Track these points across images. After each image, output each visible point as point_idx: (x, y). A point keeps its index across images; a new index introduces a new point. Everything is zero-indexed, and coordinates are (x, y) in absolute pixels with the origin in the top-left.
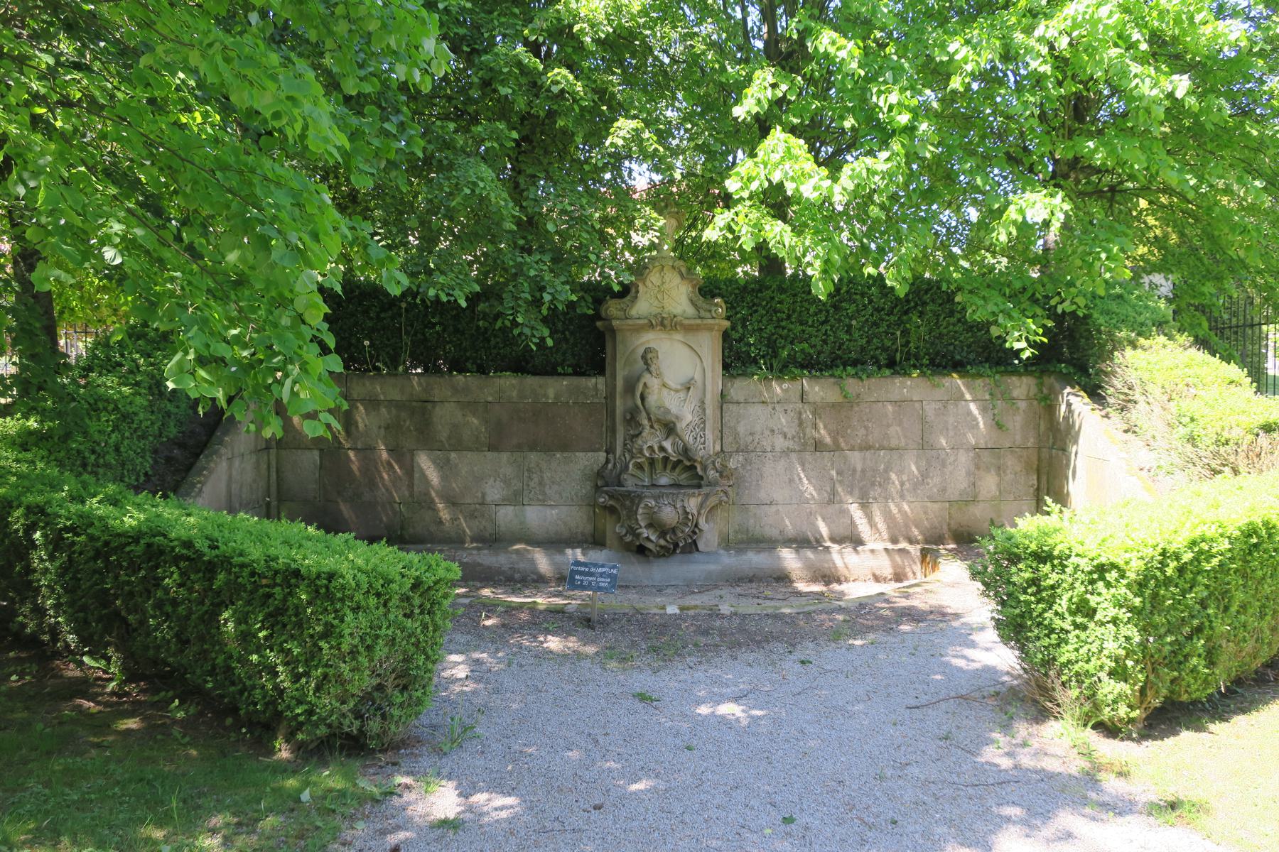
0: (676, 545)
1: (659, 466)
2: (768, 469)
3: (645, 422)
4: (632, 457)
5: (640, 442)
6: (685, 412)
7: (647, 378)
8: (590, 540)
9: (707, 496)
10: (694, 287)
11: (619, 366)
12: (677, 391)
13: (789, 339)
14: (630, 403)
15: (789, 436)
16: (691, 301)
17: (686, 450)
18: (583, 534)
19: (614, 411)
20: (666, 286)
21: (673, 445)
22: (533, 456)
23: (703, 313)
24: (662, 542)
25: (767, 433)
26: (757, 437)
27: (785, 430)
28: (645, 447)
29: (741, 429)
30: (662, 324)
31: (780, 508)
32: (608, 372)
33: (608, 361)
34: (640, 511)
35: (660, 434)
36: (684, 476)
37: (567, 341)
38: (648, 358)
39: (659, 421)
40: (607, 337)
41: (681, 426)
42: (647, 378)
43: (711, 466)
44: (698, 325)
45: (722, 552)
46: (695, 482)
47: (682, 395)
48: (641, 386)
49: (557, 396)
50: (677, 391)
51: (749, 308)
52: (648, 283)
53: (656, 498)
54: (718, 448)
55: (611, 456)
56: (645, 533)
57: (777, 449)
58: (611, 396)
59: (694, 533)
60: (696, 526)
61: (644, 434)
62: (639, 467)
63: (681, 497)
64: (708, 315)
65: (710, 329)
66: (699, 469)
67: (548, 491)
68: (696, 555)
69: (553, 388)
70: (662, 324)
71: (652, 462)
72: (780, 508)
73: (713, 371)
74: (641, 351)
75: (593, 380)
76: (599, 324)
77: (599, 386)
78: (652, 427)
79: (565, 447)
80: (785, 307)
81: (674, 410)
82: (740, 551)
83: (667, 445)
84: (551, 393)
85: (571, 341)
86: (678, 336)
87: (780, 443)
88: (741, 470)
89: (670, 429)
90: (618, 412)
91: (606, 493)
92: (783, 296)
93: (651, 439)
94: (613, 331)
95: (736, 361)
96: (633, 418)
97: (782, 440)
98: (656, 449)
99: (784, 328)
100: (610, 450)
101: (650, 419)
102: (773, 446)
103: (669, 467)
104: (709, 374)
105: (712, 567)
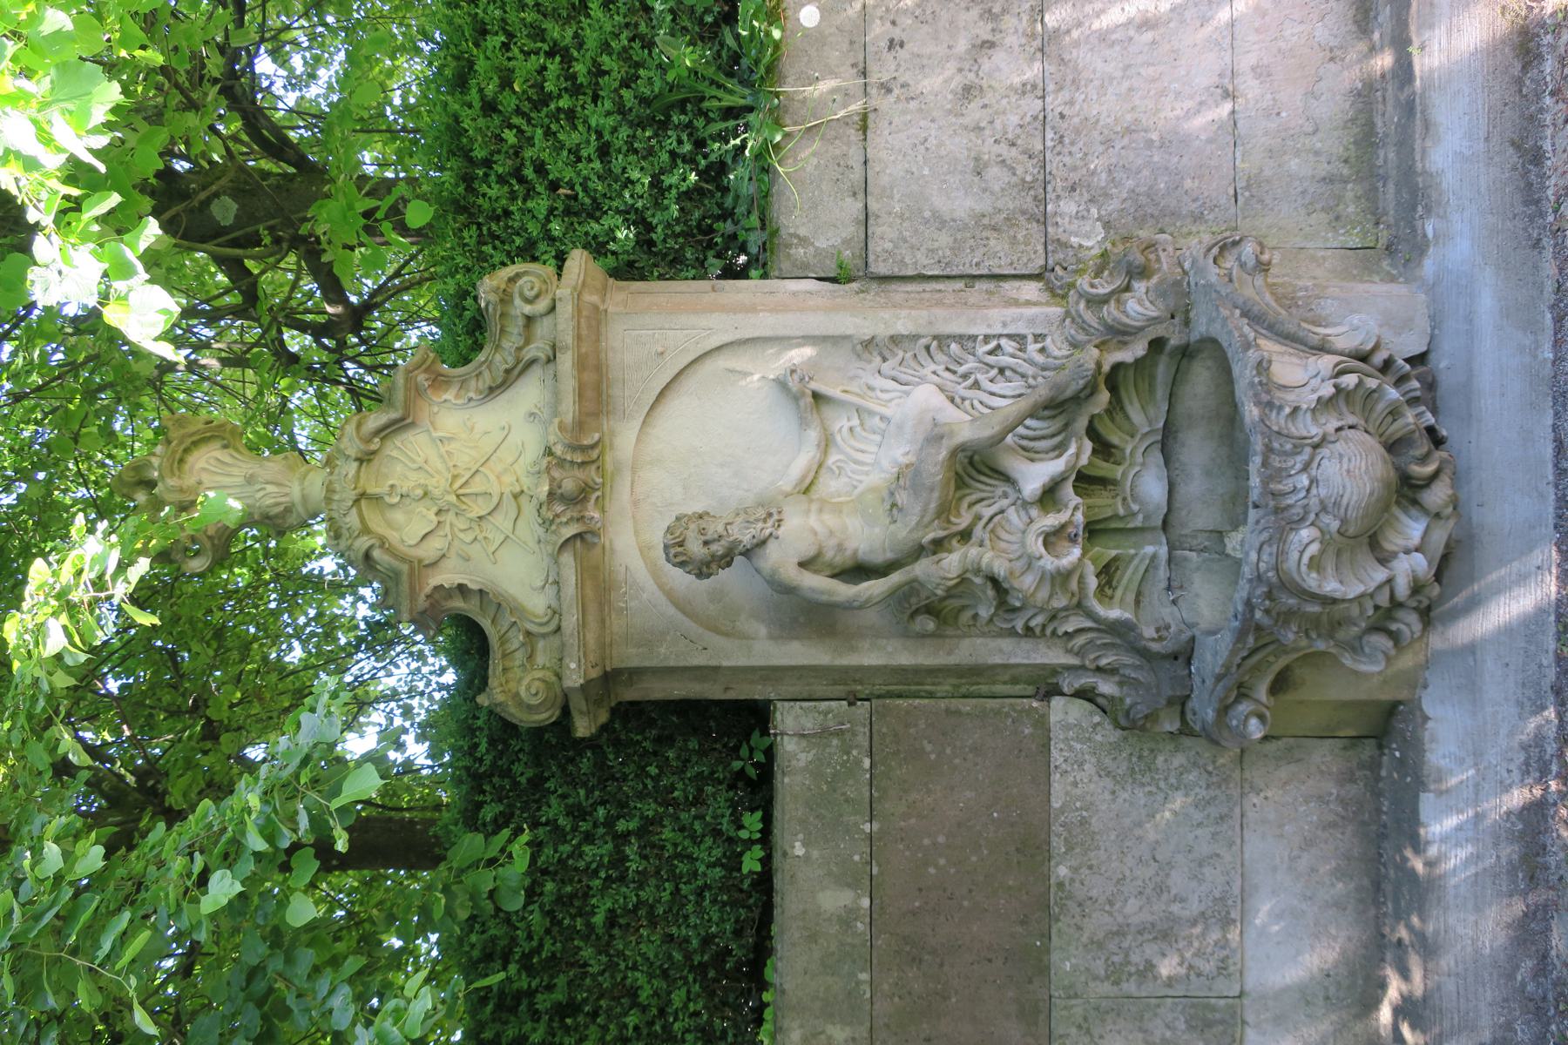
0: (1431, 430)
1: (1107, 505)
2: (1105, 107)
3: (952, 562)
4: (1080, 607)
5: (1028, 582)
6: (904, 416)
7: (782, 558)
8: (1368, 750)
9: (1253, 317)
10: (439, 382)
11: (733, 655)
12: (827, 443)
13: (638, 53)
14: (871, 617)
15: (984, 31)
16: (493, 391)
17: (1058, 407)
18: (1348, 778)
19: (901, 672)
20: (438, 484)
21: (1031, 454)
22: (1066, 962)
23: (537, 349)
24: (1437, 495)
25: (974, 113)
26: (989, 149)
27: (962, 45)
28: (1049, 563)
29: (962, 205)
30: (579, 498)
31: (1246, 62)
32: (757, 692)
33: (714, 691)
34: (1331, 587)
35: (990, 503)
36: (1135, 413)
37: (648, 826)
38: (708, 555)
39: (945, 511)
40: (630, 695)
41: (966, 428)
42: (782, 558)
43: (1110, 311)
44: (581, 364)
45: (1429, 266)
46: (1163, 369)
47: (841, 423)
48: (815, 582)
49: (846, 878)
50: (827, 443)
51: (530, 193)
52: (430, 550)
53: (1284, 520)
54: (1031, 290)
55: (1068, 683)
56: (1410, 567)
57: (1033, 72)
58: (852, 687)
59: (1387, 365)
60: (1364, 358)
61: (1000, 568)
62: (1108, 573)
63: (1277, 421)
64: (542, 329)
65: (593, 322)
66: (1127, 356)
67: (1194, 907)
68: (1440, 363)
69: (818, 891)
70: (579, 498)
71: (1094, 531)
72: (1246, 62)
73: (752, 309)
74: (680, 579)
75: (788, 746)
76: (583, 728)
77: (810, 724)
78: (965, 536)
79: (1031, 848)
80: (525, 68)
81: (900, 452)
82: (1416, 194)
83: (1034, 476)
84: (834, 900)
85: (650, 809)
86: (625, 438)
87: (1012, 68)
88: (1113, 205)
89: (975, 467)
90: (905, 659)
91: (1224, 710)
92: (481, 65)
93: (1019, 540)
94: (610, 678)
95: (715, 234)
97: (999, 57)
98: (1052, 520)
99: (598, 72)
100: (1047, 686)
101: (938, 545)
102: (1025, 89)
103: (1104, 468)
104: (765, 324)
105: (1486, 302)
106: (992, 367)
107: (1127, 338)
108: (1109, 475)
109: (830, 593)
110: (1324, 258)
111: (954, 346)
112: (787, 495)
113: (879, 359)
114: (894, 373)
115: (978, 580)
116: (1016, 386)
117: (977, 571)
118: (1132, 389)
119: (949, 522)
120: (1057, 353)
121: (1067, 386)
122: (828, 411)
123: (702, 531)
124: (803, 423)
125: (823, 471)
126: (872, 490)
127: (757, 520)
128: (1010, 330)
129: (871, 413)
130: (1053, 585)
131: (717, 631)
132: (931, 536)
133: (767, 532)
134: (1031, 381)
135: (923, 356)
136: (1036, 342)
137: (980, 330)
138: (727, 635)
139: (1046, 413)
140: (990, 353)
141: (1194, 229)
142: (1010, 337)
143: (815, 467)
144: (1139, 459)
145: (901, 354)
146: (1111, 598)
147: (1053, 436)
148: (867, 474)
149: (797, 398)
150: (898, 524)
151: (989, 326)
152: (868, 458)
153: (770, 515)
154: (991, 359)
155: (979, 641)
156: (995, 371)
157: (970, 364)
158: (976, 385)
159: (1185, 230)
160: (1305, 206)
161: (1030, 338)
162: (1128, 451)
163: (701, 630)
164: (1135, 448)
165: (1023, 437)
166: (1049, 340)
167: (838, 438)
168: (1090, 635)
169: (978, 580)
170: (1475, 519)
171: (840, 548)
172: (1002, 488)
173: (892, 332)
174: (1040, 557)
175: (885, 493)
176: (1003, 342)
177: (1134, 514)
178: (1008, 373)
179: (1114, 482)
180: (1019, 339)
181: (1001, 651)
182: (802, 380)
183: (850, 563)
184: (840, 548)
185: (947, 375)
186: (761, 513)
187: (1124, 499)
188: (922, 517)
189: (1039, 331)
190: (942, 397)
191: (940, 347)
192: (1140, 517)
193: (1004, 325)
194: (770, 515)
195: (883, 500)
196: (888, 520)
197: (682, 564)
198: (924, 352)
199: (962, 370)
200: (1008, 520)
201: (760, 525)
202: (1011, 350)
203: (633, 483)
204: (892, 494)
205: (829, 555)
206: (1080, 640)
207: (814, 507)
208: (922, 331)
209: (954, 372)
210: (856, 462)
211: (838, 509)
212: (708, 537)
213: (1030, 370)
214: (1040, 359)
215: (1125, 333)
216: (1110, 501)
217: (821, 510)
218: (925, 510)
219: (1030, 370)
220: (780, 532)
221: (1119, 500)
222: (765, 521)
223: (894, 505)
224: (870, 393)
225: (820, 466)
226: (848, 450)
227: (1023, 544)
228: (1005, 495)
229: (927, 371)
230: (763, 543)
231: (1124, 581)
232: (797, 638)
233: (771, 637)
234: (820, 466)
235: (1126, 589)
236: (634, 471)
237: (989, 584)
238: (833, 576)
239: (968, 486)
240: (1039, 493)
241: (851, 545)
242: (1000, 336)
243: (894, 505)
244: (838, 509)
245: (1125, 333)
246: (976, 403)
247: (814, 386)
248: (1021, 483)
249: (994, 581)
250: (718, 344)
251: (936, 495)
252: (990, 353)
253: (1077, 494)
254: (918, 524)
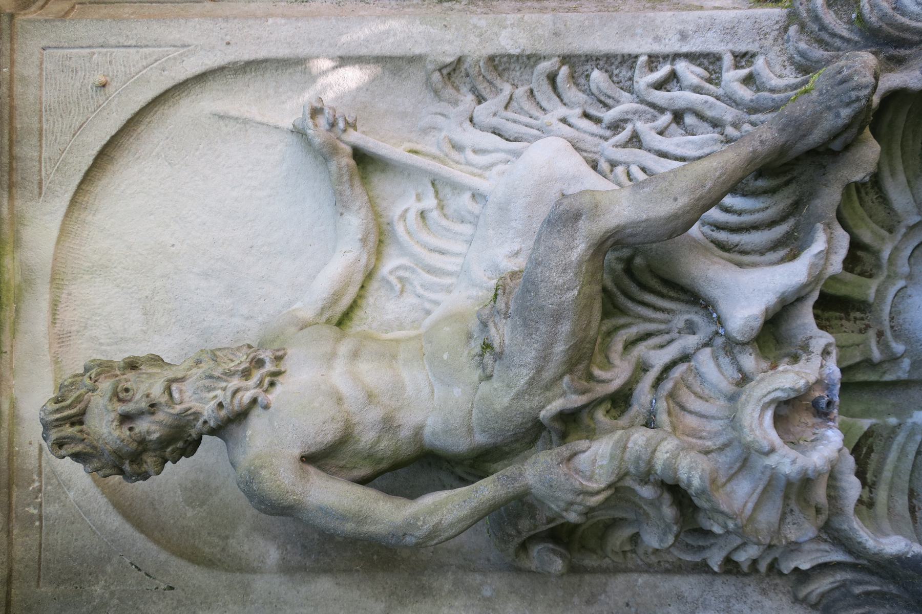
12: (380, 238)
28: (788, 462)
35: (659, 344)
39: (582, 359)
41: (624, 207)
42: (273, 444)
47: (404, 203)
50: (380, 238)
61: (692, 470)
81: (507, 251)
83: (748, 292)
89: (637, 275)
96: (562, 536)
106: (662, 110)
107: (903, 52)
108: (856, 294)
109: (360, 519)
111: (597, 76)
112: (304, 326)
113: (470, 98)
114: (495, 121)
115: (647, 492)
116: (704, 139)
117: (646, 477)
118: (899, 153)
119: (590, 377)
120: (775, 82)
121: (815, 122)
122: (383, 185)
123: (118, 395)
124: (341, 204)
125: (374, 285)
126: (452, 318)
127: (230, 374)
128: (694, 46)
129: (457, 187)
130: (786, 497)
131: (194, 557)
132: (556, 405)
133: (246, 397)
134: (730, 131)
135: (544, 93)
136: (737, 67)
137: (642, 46)
138: (209, 563)
139: (761, 183)
140: (659, 86)
142: (691, 57)
143: (359, 278)
144: (906, 269)
145: (507, 89)
147: (772, 224)
148: (448, 289)
149: (324, 154)
150: (495, 383)
151: (657, 39)
152: (448, 263)
153: (260, 363)
154: (660, 97)
155: (642, 579)
156: (667, 118)
157: (626, 105)
158: (635, 140)
161: (728, 60)
162: (886, 254)
163: (163, 556)
164: (896, 249)
165: (719, 227)
166: (760, 62)
167: (400, 229)
168: (840, 576)
169: (647, 492)
171: (388, 425)
172: (684, 315)
173: (490, 50)
174: (772, 450)
175: (474, 325)
176: (682, 67)
177: (894, 359)
178: (689, 120)
179: (863, 306)
180: (709, 61)
181: (680, 597)
182: (333, 125)
183: (407, 450)
184: (388, 425)
185: (586, 124)
186: (242, 360)
187: (880, 334)
188: (539, 370)
189: (742, 48)
190: (577, 159)
191: (573, 77)
192: (906, 363)
193: (684, 36)
194: (260, 363)
195: (470, 336)
196: (477, 374)
197: (76, 457)
198: (546, 87)
199: (609, 116)
200: (698, 374)
201: (235, 382)
202: (695, 80)
203: (55, 305)
204: (484, 325)
205: (366, 438)
206: (822, 585)
207: (344, 348)
208: (541, 48)
209: (598, 121)
210: (431, 270)
211: (389, 353)
212: (129, 407)
213: (729, 114)
214: (746, 94)
215: (900, 43)
216: (857, 338)
217: (355, 355)
218: (544, 358)
219: (729, 114)
220: (273, 397)
221: (872, 333)
222: (246, 374)
223: (487, 346)
224: (454, 154)
225: (369, 275)
226: (417, 249)
227: (733, 421)
228: (691, 328)
229: (551, 118)
230: (241, 416)
231: (887, 474)
232: (327, 570)
233: (287, 569)
234: (369, 275)
235: (892, 487)
236: (57, 280)
237: (667, 497)
238: (364, 481)
239: (623, 312)
240: (758, 324)
241: (409, 420)
242: (676, 56)
243: (487, 346)
244: (389, 353)
245: (900, 43)
246: (635, 170)
247: (355, 137)
248: (724, 308)
249: (676, 492)
250: (198, 70)
251: (565, 328)
252: (659, 86)
253: (821, 327)
254: (530, 383)
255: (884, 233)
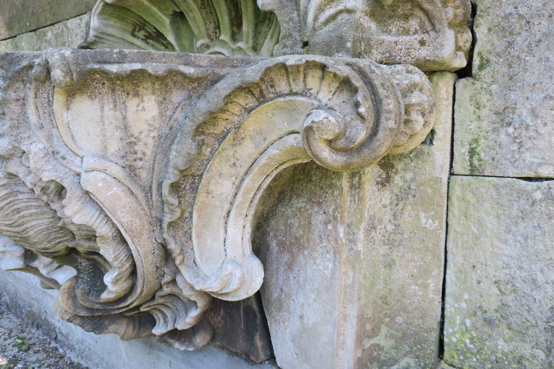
110: (425, 286)
141: (484, 112)
146: (133, 35)
159: (484, 98)
160: (511, 281)
170: (162, 355)
255: (251, 44)
